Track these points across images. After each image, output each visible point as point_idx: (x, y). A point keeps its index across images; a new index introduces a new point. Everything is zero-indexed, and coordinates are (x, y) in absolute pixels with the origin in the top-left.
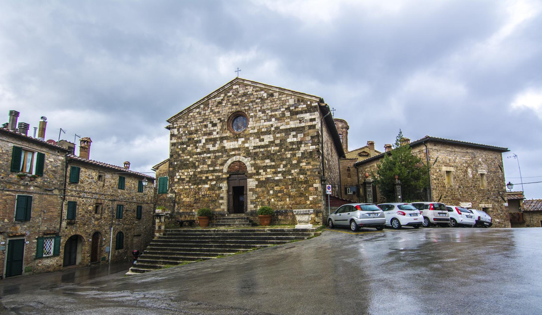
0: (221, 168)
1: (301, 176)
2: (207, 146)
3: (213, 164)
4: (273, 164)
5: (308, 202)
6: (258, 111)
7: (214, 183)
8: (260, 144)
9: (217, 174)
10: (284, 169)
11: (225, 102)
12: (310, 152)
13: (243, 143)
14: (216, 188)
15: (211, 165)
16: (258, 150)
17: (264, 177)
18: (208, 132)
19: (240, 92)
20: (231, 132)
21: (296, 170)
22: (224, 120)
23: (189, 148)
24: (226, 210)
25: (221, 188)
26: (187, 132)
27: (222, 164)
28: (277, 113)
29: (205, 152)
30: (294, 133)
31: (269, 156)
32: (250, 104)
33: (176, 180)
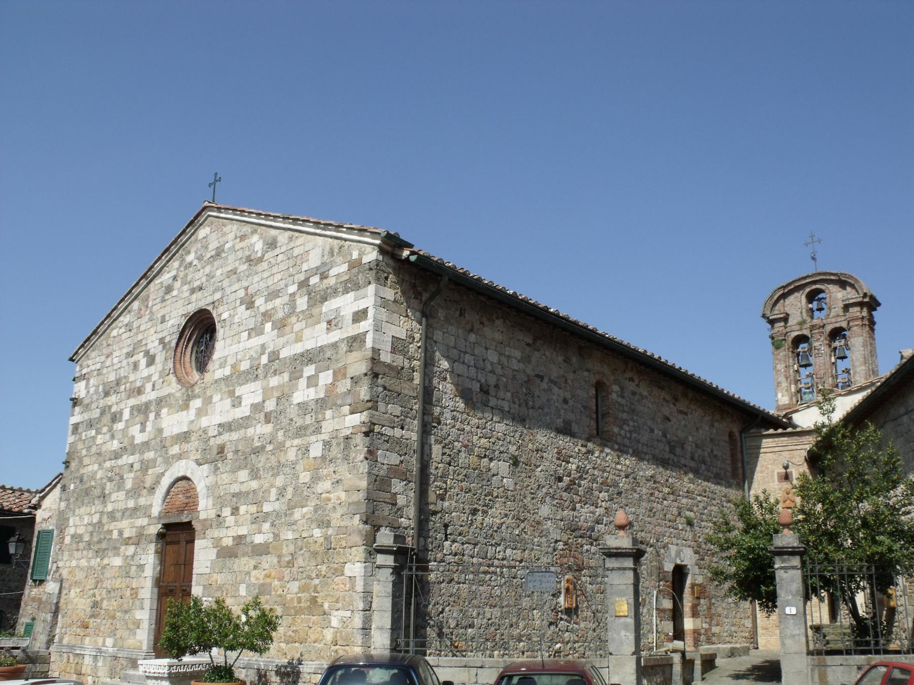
1: (317, 533)
3: (135, 492)
4: (254, 484)
5: (329, 635)
6: (238, 302)
10: (277, 506)
11: (177, 284)
12: (347, 438)
13: (200, 412)
16: (226, 437)
19: (211, 247)
20: (179, 380)
22: (170, 342)
23: (100, 439)
24: (145, 647)
27: (152, 489)
30: (309, 370)
31: (249, 456)
33: (68, 540)
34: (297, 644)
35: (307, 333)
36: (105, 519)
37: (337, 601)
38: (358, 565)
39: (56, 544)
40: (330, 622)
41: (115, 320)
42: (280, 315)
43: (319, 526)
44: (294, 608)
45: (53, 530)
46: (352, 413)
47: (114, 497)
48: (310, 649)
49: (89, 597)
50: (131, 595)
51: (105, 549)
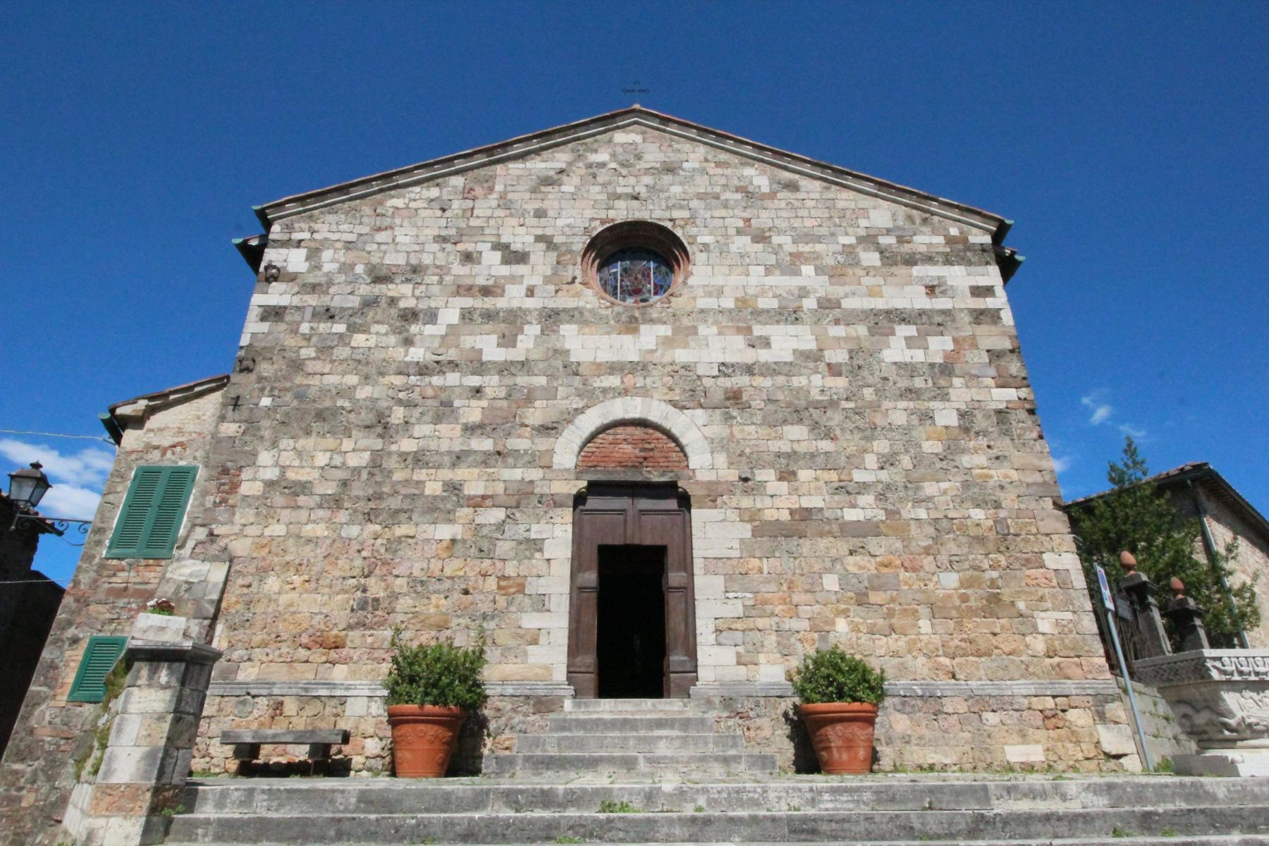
0: (543, 444)
1: (978, 514)
2: (468, 342)
4: (826, 445)
5: (1039, 645)
6: (732, 232)
7: (494, 515)
8: (749, 356)
9: (517, 474)
10: (884, 476)
12: (999, 412)
13: (667, 342)
14: (503, 548)
15: (481, 426)
16: (741, 381)
18: (481, 281)
19: (647, 157)
21: (944, 485)
24: (560, 674)
25: (535, 545)
26: (360, 269)
27: (549, 429)
28: (819, 248)
29: (454, 365)
30: (911, 330)
32: (695, 204)
33: (250, 487)
34: (971, 658)
36: (391, 463)
37: (1042, 599)
38: (1069, 555)
39: (204, 493)
40: (1035, 627)
41: (397, 187)
42: (830, 261)
43: (978, 506)
44: (957, 608)
45: (195, 469)
46: (998, 386)
47: (419, 430)
48: (1006, 663)
49: (344, 591)
50: (499, 588)
51: (397, 512)
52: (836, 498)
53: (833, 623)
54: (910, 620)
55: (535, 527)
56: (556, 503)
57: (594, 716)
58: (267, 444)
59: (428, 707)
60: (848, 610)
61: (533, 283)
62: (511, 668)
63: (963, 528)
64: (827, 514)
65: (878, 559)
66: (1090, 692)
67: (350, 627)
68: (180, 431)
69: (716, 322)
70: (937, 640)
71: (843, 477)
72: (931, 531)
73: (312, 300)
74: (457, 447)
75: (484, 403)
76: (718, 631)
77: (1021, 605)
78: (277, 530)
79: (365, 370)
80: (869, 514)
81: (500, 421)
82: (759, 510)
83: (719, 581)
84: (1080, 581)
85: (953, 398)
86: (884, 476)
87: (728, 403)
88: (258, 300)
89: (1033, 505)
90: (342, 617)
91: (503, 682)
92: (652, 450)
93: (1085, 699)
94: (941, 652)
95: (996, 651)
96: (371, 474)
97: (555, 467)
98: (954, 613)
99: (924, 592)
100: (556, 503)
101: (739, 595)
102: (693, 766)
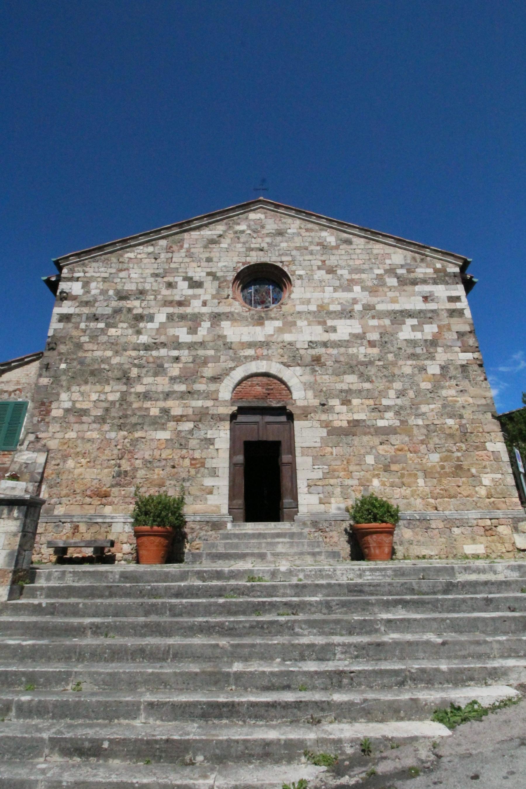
0: (213, 387)
1: (450, 422)
2: (172, 331)
4: (367, 385)
5: (483, 492)
6: (315, 268)
8: (325, 337)
9: (199, 403)
10: (399, 402)
12: (463, 366)
13: (280, 330)
14: (193, 443)
15: (179, 377)
16: (321, 351)
17: (341, 417)
18: (177, 298)
19: (267, 227)
21: (432, 406)
24: (225, 510)
25: (210, 442)
26: (111, 292)
27: (216, 379)
28: (363, 276)
29: (164, 345)
30: (415, 321)
32: (294, 253)
33: (56, 412)
35: (401, 299)
37: (485, 467)
38: (500, 444)
39: (32, 416)
40: (481, 482)
41: (130, 246)
42: (370, 284)
43: (450, 417)
44: (439, 473)
45: (27, 403)
46: (463, 352)
47: (146, 380)
48: (465, 501)
49: (108, 467)
50: (191, 464)
51: (136, 424)
52: (373, 414)
53: (371, 482)
54: (413, 480)
55: (210, 432)
56: (221, 418)
57: (244, 532)
58: (65, 389)
59: (155, 528)
60: (380, 474)
61: (205, 298)
62: (199, 507)
63: (442, 430)
64: (368, 423)
65: (396, 447)
66: (510, 516)
67: (112, 486)
68: (18, 383)
69: (306, 319)
70: (427, 489)
71: (377, 403)
72: (425, 431)
73: (86, 310)
74: (167, 389)
75: (181, 365)
76: (309, 486)
77: (473, 471)
78: (72, 435)
79: (116, 348)
80: (391, 422)
81: (189, 375)
82: (331, 421)
83: (310, 459)
84: (505, 457)
85: (437, 358)
86: (399, 402)
87: (313, 363)
88: (57, 310)
89: (481, 416)
90: (108, 481)
91: (195, 514)
92: (272, 389)
93: (508, 520)
94: (429, 496)
95: (460, 495)
96: (121, 405)
97: (220, 399)
98: (437, 475)
99: (421, 464)
100: (221, 418)
101: (320, 467)
102: (296, 557)
